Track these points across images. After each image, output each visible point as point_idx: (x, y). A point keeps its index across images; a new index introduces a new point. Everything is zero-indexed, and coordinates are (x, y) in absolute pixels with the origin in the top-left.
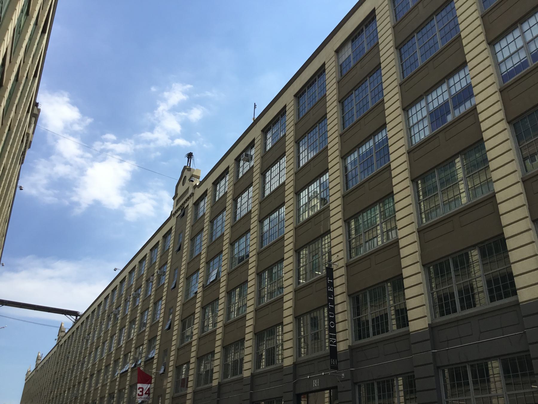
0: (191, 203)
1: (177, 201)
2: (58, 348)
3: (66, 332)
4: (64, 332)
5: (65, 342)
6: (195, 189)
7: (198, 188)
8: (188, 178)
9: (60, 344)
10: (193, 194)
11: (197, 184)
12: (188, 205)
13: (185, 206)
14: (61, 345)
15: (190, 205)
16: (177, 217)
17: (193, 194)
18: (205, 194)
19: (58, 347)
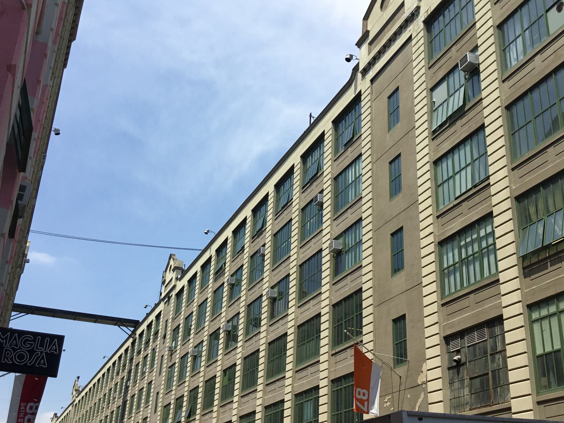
0: (174, 293)
1: (166, 287)
2: (72, 409)
3: (81, 390)
4: (78, 390)
5: (79, 401)
6: (177, 280)
7: (180, 281)
8: (172, 268)
9: (75, 403)
10: (174, 287)
11: (179, 277)
12: (172, 295)
13: (170, 295)
14: (76, 405)
15: (173, 296)
16: (165, 303)
17: (174, 287)
18: (182, 290)
19: (73, 406)
